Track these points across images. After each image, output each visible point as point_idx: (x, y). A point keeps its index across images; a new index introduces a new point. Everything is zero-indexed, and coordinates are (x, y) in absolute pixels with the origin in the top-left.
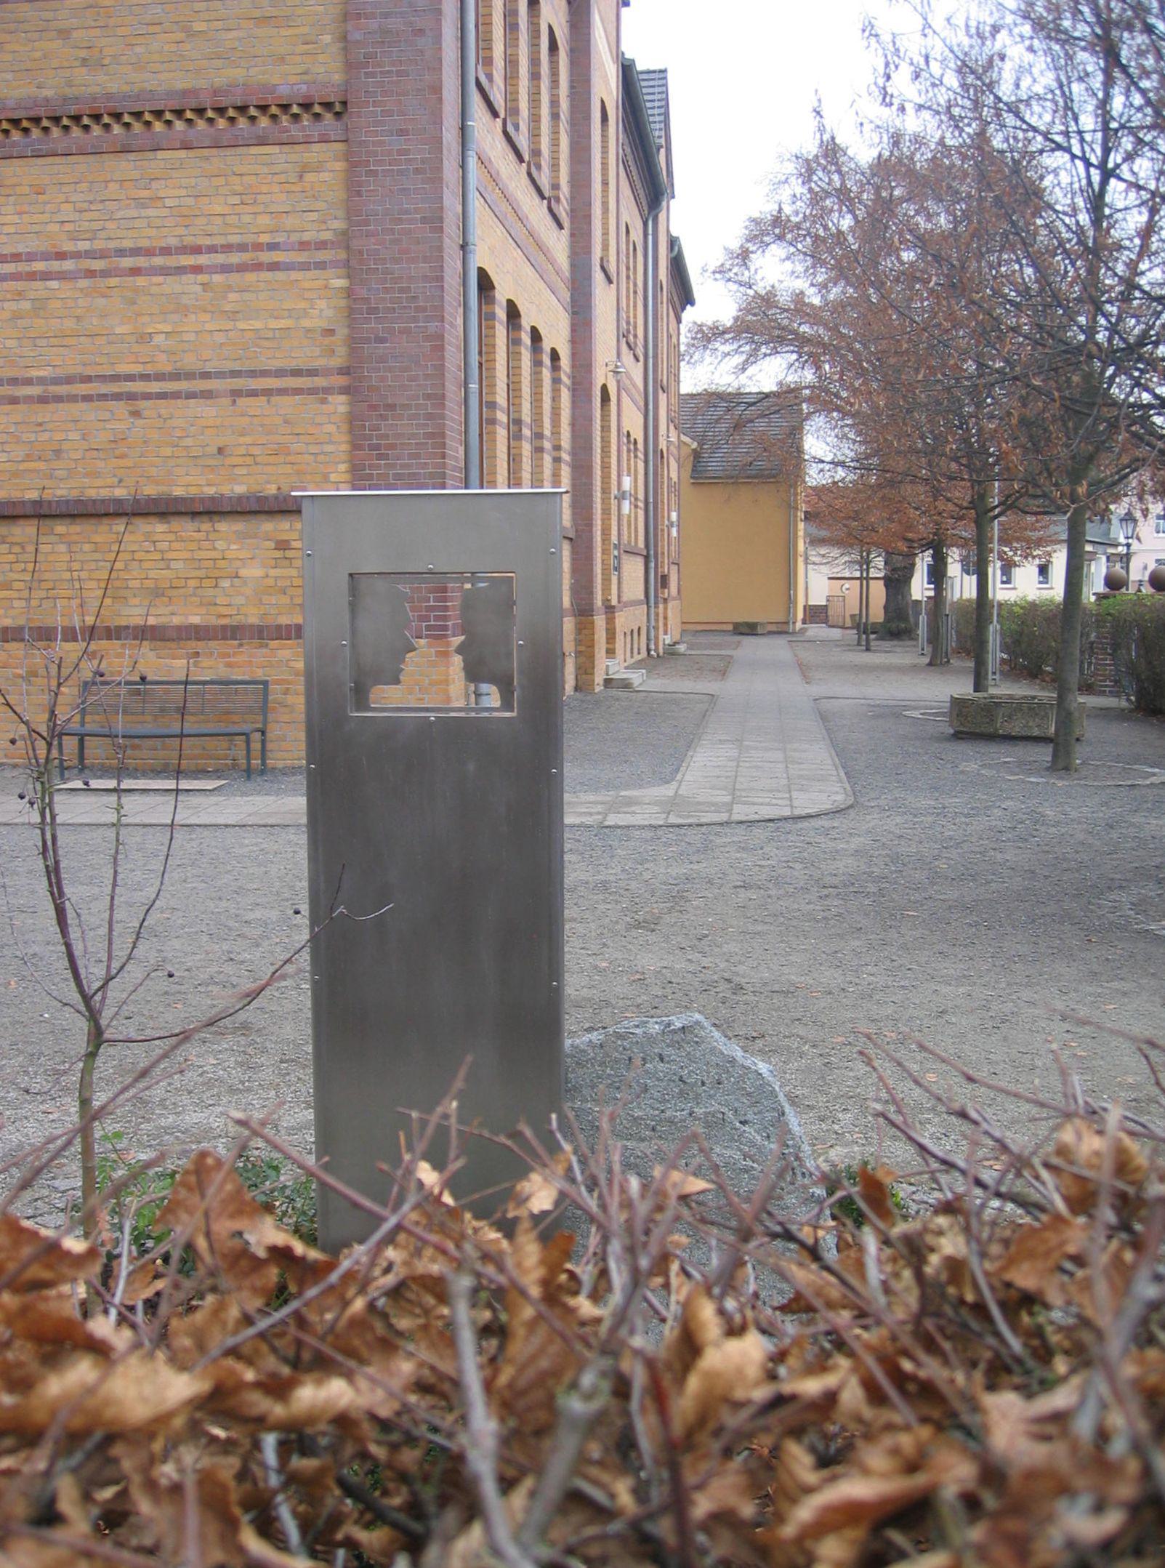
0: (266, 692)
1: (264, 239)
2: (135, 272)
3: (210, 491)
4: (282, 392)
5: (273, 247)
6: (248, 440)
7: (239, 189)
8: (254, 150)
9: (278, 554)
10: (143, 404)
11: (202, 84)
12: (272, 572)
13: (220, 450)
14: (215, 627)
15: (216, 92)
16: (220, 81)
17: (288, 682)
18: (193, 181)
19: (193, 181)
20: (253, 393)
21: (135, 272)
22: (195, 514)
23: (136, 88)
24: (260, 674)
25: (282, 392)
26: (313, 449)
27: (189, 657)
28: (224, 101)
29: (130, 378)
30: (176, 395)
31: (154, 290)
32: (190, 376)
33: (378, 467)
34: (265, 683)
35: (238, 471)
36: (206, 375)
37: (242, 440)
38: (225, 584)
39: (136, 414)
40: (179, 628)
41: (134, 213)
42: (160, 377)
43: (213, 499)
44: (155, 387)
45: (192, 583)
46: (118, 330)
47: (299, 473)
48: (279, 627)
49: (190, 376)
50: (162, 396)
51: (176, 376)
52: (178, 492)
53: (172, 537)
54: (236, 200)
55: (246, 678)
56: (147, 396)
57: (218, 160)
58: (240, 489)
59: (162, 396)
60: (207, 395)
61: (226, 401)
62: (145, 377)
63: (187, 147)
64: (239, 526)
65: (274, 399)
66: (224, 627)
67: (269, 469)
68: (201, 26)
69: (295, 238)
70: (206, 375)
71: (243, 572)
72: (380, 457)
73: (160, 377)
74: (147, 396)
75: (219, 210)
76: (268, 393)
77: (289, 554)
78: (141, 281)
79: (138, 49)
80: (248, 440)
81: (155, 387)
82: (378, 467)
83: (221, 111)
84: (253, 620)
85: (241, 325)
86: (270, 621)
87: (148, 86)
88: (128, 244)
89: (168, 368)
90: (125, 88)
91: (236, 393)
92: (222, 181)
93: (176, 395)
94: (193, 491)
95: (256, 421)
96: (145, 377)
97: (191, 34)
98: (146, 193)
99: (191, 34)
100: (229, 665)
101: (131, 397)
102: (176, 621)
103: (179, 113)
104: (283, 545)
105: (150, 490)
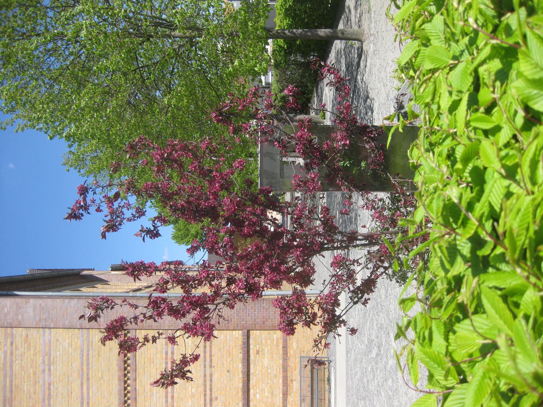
0: (303, 357)
1: (164, 356)
2: (173, 397)
3: (241, 375)
4: (211, 351)
5: (167, 353)
6: (225, 362)
7: (149, 363)
9: (261, 353)
10: (214, 396)
11: (117, 374)
12: (266, 355)
13: (228, 372)
14: (283, 374)
15: (119, 370)
16: (116, 368)
17: (300, 351)
18: (146, 378)
19: (146, 378)
20: (211, 361)
21: (173, 397)
22: (248, 380)
23: (117, 395)
24: (298, 360)
25: (211, 351)
26: (228, 342)
27: (292, 383)
28: (123, 367)
29: (205, 400)
30: (211, 385)
31: (178, 391)
32: (205, 381)
33: (234, 321)
34: (301, 357)
35: (235, 366)
36: (205, 376)
37: (225, 365)
38: (270, 370)
39: (216, 398)
40: (283, 386)
41: (155, 397)
42: (205, 391)
43: (243, 374)
44: (208, 392)
45: (269, 381)
46: (190, 404)
47: (235, 346)
48: (283, 354)
49: (205, 381)
50: (211, 390)
51: (205, 386)
52: (241, 385)
53: (255, 388)
54: (152, 364)
55: (299, 364)
56: (211, 395)
57: (139, 370)
58: (240, 365)
59: (211, 390)
60: (211, 375)
61: (213, 369)
62: (205, 395)
63: (135, 380)
64: (252, 366)
65: (213, 354)
66: (283, 371)
67: (234, 357)
68: (100, 375)
69: (164, 347)
70: (205, 376)
71: (266, 365)
72: (231, 321)
73: (205, 391)
74: (211, 395)
75: (154, 370)
76: (211, 356)
77: (260, 350)
78: (175, 396)
79: (106, 394)
80: (225, 362)
81: (208, 392)
82: (234, 321)
83: (125, 369)
84: (281, 362)
86: (281, 357)
87: (117, 392)
88: (164, 400)
89: (203, 388)
90: (117, 398)
91: (211, 366)
92: (146, 369)
93: (211, 385)
94: (241, 381)
95: (219, 360)
96: (205, 395)
97: (102, 377)
98: (149, 393)
99: (102, 377)
100: (295, 370)
101: (211, 400)
102: (281, 387)
103: (125, 382)
104: (258, 352)
105: (240, 394)
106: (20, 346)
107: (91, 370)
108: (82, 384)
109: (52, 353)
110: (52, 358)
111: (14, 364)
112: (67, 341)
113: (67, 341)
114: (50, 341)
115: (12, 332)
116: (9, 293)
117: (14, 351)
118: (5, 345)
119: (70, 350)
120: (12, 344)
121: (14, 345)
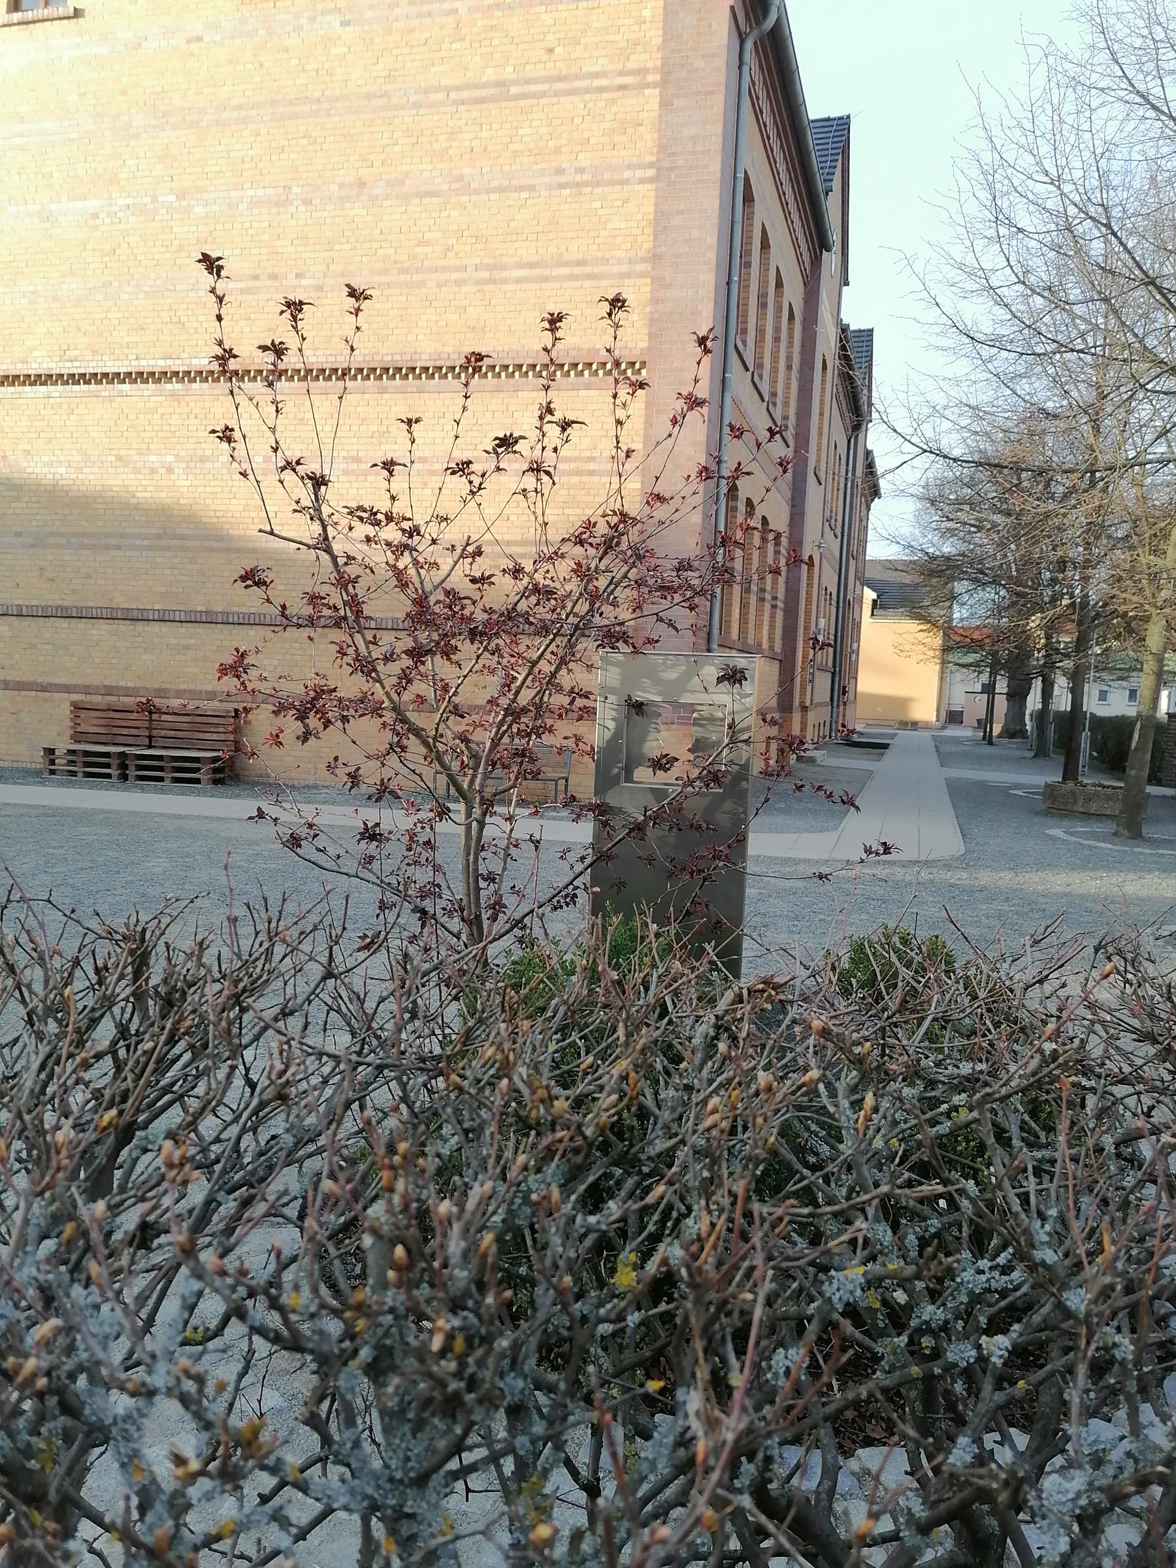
8: (582, 393)
85: (567, 511)
106: (614, 109)
107: (557, 285)
108: (531, 265)
109: (599, 190)
110: (589, 190)
111: (576, 98)
112: (623, 225)
113: (623, 225)
114: (625, 182)
115: (648, 86)
116: (746, 69)
117: (605, 96)
118: (621, 73)
119: (606, 233)
120: (623, 87)
121: (620, 94)
